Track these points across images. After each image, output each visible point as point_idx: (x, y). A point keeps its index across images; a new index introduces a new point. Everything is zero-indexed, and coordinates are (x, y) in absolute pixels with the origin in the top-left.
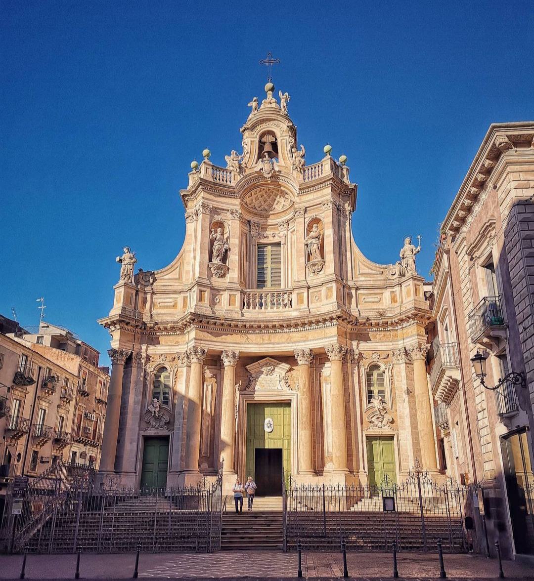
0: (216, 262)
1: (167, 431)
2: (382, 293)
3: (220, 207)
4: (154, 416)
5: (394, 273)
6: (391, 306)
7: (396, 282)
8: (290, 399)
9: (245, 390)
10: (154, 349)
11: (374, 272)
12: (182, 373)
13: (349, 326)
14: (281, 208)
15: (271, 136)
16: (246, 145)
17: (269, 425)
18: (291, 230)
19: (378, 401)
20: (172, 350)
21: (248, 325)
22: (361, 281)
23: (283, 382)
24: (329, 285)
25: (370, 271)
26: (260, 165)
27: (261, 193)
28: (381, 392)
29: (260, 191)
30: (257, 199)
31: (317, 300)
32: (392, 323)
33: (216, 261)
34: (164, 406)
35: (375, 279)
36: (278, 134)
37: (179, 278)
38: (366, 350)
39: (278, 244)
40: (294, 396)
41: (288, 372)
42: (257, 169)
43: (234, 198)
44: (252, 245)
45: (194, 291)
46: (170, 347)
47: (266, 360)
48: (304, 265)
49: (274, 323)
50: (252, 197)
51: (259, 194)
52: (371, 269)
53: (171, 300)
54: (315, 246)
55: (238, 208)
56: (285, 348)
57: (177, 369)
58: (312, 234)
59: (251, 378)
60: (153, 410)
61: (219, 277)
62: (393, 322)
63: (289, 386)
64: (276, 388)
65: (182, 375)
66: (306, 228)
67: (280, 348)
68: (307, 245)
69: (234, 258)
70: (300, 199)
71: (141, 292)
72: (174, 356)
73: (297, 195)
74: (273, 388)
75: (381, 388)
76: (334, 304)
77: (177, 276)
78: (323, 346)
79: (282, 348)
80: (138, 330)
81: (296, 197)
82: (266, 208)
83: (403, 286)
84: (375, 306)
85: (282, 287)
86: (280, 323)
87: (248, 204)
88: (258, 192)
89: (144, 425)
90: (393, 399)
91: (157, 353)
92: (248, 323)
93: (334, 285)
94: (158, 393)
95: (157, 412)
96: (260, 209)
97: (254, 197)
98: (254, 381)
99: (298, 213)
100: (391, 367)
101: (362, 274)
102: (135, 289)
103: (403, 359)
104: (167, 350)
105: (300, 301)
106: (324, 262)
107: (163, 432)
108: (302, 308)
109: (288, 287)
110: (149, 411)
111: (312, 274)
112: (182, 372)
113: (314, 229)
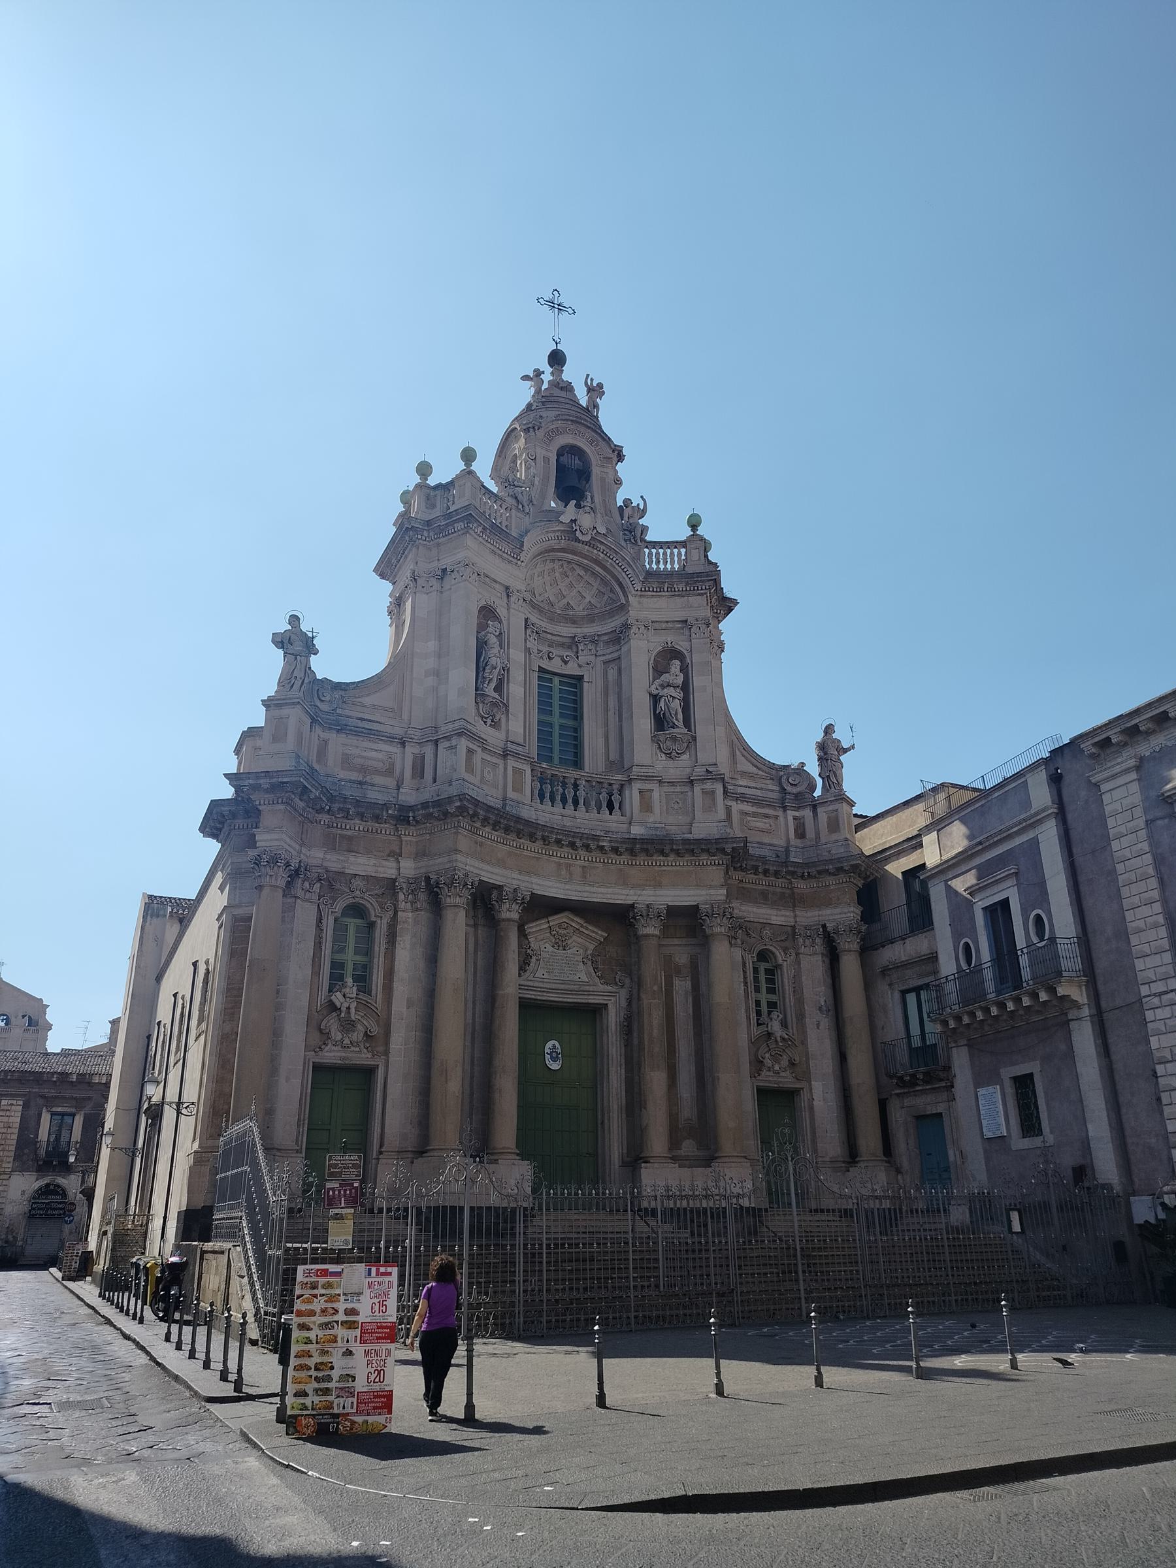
1: (369, 1055)
3: (493, 576)
8: (605, 1002)
11: (760, 773)
14: (581, 608)
15: (577, 458)
17: (554, 1055)
18: (604, 658)
20: (380, 869)
22: (741, 786)
25: (754, 770)
33: (489, 690)
35: (764, 786)
52: (756, 766)
53: (380, 756)
56: (613, 896)
57: (391, 913)
58: (665, 677)
60: (346, 1005)
66: (652, 661)
68: (655, 699)
74: (571, 978)
75: (773, 998)
76: (711, 824)
78: (696, 904)
83: (820, 810)
86: (613, 844)
89: (316, 1038)
91: (347, 871)
95: (353, 1010)
96: (541, 599)
98: (534, 959)
101: (744, 774)
103: (820, 946)
105: (646, 806)
106: (694, 738)
107: (363, 1058)
108: (651, 820)
110: (332, 1007)
113: (673, 670)
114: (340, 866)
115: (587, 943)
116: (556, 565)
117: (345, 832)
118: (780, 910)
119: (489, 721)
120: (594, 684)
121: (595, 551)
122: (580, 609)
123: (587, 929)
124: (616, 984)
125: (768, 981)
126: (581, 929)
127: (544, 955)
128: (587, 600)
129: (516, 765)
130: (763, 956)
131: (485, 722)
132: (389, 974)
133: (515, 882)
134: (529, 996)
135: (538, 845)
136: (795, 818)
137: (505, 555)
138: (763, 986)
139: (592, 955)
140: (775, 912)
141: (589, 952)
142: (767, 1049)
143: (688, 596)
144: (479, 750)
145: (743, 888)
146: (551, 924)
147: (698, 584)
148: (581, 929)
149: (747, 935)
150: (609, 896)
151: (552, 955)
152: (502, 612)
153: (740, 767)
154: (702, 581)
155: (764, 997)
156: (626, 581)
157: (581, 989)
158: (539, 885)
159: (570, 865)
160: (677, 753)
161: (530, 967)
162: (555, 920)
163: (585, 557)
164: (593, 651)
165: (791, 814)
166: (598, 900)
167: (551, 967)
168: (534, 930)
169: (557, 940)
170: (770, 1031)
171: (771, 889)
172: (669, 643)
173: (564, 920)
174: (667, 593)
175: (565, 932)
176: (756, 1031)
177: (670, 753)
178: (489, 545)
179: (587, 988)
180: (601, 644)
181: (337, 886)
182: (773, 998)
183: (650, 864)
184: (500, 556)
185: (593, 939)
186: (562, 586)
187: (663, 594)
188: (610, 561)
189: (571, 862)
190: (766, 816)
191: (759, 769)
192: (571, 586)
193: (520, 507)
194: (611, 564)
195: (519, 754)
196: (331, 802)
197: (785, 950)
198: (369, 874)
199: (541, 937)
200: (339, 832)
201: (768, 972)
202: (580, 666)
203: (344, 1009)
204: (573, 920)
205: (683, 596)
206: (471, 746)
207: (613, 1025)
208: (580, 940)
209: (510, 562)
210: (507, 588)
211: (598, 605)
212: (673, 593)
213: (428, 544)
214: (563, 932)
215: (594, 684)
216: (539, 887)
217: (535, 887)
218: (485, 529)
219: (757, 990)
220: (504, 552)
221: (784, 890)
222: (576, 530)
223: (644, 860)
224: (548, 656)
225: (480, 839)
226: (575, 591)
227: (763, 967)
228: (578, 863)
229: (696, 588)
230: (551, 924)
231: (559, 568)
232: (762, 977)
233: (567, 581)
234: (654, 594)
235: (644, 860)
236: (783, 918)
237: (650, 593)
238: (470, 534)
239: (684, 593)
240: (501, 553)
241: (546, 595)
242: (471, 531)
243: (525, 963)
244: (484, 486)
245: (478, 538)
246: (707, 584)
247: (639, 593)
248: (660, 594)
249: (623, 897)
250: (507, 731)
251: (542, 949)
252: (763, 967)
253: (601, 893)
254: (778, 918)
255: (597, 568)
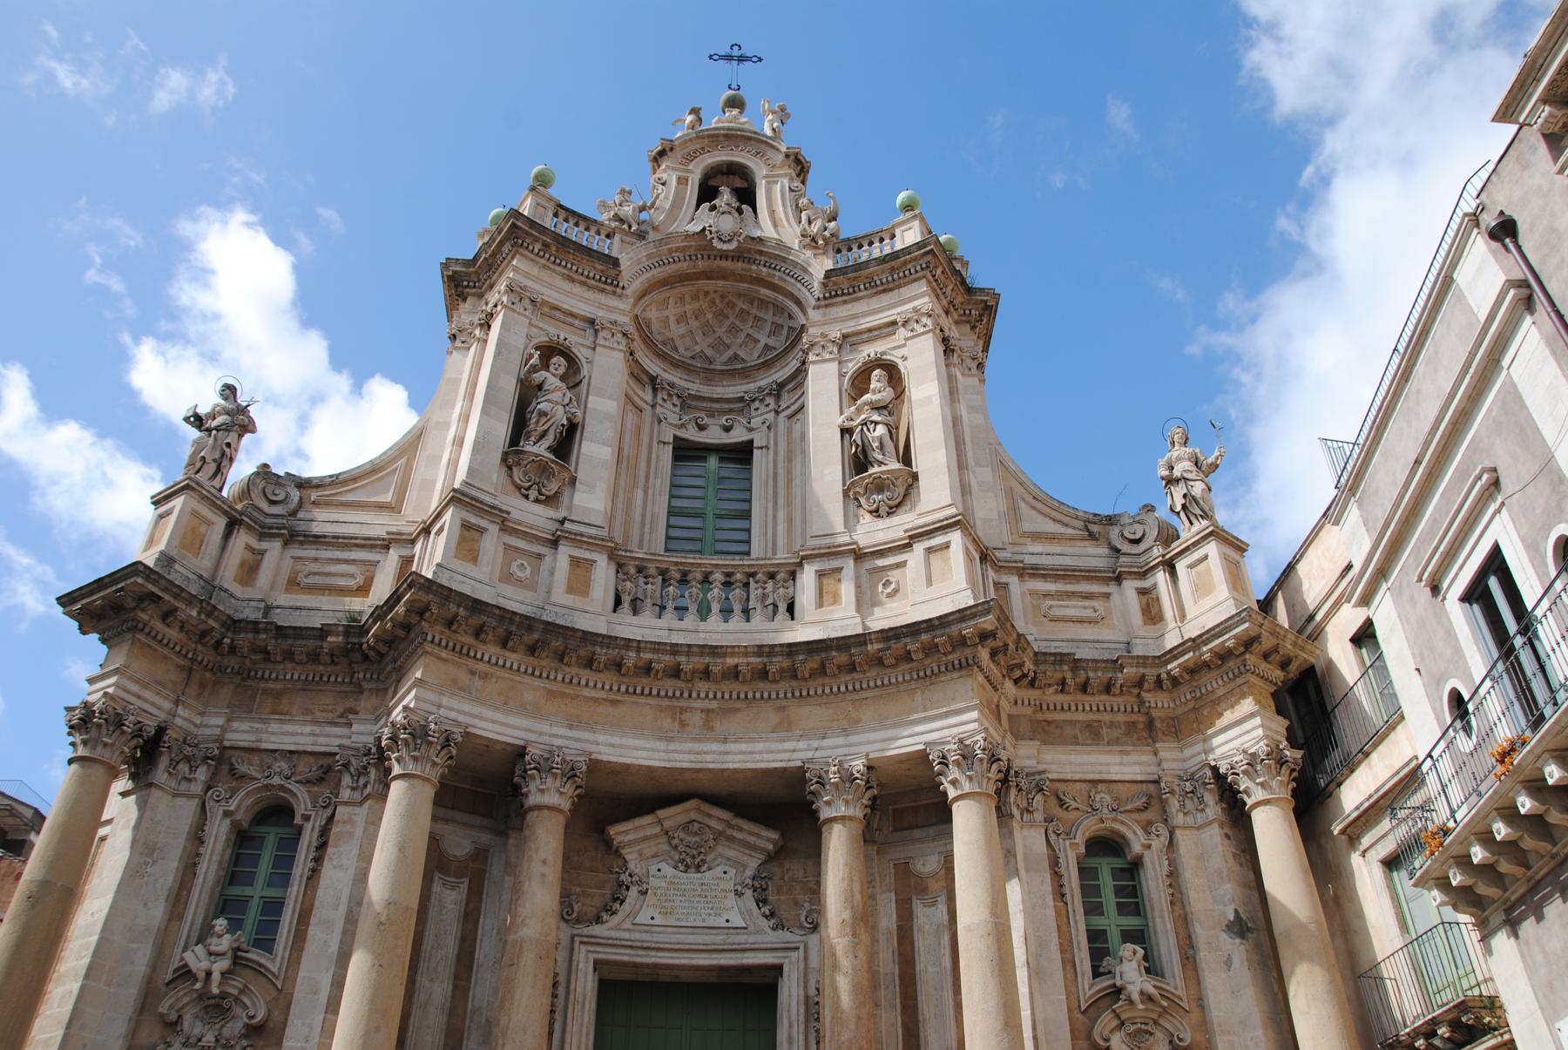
0: (535, 449)
2: (1107, 596)
4: (204, 995)
5: (1137, 536)
6: (1141, 633)
7: (1157, 551)
9: (598, 920)
10: (257, 731)
11: (1070, 531)
12: (348, 827)
13: (1009, 685)
14: (755, 356)
16: (663, 184)
19: (1134, 964)
20: (322, 740)
21: (631, 658)
23: (749, 898)
24: (938, 540)
25: (1058, 528)
26: (705, 219)
27: (696, 305)
28: (1137, 936)
29: (695, 297)
30: (682, 318)
31: (889, 596)
32: (1159, 682)
33: (539, 449)
34: (255, 955)
36: (759, 171)
37: (393, 508)
38: (1069, 777)
39: (742, 454)
40: (794, 955)
41: (772, 858)
42: (695, 227)
43: (614, 293)
44: (659, 442)
45: (441, 530)
46: (317, 729)
47: (687, 811)
48: (839, 488)
49: (730, 661)
50: (667, 313)
51: (690, 307)
54: (881, 430)
55: (625, 320)
56: (766, 756)
57: (329, 811)
59: (624, 877)
60: (205, 964)
61: (537, 501)
62: (1164, 676)
63: (772, 915)
64: (721, 922)
65: (351, 835)
67: (749, 757)
68: (846, 432)
69: (594, 451)
70: (824, 315)
71: (250, 528)
72: (326, 761)
73: (813, 303)
74: (711, 922)
77: (387, 497)
78: (921, 747)
79: (757, 757)
80: (206, 655)
81: (811, 312)
82: (709, 352)
83: (1180, 566)
84: (1087, 632)
85: (757, 549)
87: (654, 328)
88: (688, 298)
90: (1189, 958)
91: (265, 746)
92: (632, 654)
93: (956, 537)
94: (244, 902)
95: (216, 976)
96: (689, 354)
97: (672, 312)
98: (634, 891)
99: (817, 349)
100: (1164, 839)
101: (1037, 537)
102: (225, 513)
103: (1213, 808)
104: (302, 740)
106: (915, 477)
108: (836, 616)
109: (774, 553)
110: (185, 973)
111: (868, 516)
112: (349, 821)
114: (253, 739)
115: (745, 858)
116: (703, 303)
117: (271, 685)
118: (1127, 753)
119: (533, 494)
120: (771, 451)
121: (754, 267)
122: (752, 356)
123: (740, 829)
124: (802, 927)
125: (1118, 891)
126: (729, 832)
127: (654, 882)
128: (761, 344)
129: (578, 553)
130: (1106, 845)
131: (527, 497)
132: (304, 917)
133: (546, 739)
134: (618, 958)
135: (609, 678)
136: (1142, 592)
137: (592, 282)
138: (1109, 899)
139: (754, 878)
140: (1117, 759)
141: (749, 872)
142: (1115, 1023)
143: (899, 287)
144: (493, 529)
145: (1049, 722)
146: (667, 824)
147: (909, 266)
148: (729, 832)
149: (1062, 806)
150: (757, 757)
151: (672, 883)
152: (581, 353)
153: (1027, 527)
154: (915, 259)
155: (1112, 922)
156: (804, 294)
157: (730, 941)
158: (612, 745)
159: (683, 710)
160: (891, 508)
161: (626, 906)
162: (672, 816)
163: (742, 279)
164: (772, 406)
165: (1130, 586)
166: (737, 766)
167: (670, 904)
168: (631, 837)
169: (684, 855)
170: (1118, 983)
171: (1106, 717)
172: (872, 355)
173: (693, 816)
174: (865, 293)
175: (697, 839)
176: (1088, 988)
177: (877, 511)
178: (558, 269)
179: (743, 938)
180: (785, 396)
181: (243, 768)
182: (1131, 922)
183: (835, 689)
184: (583, 284)
185: (754, 848)
186: (721, 331)
187: (861, 294)
188: (778, 274)
189: (683, 703)
190: (1088, 596)
191: (1066, 525)
192: (734, 330)
193: (625, 226)
194: (780, 278)
195: (582, 535)
196: (235, 632)
197: (1147, 827)
198: (301, 748)
199: (648, 852)
200: (262, 685)
201: (1117, 873)
202: (750, 430)
203: (202, 975)
204: (710, 816)
205: (891, 290)
206: (474, 520)
207: (794, 1004)
208: (731, 853)
209: (603, 291)
210: (592, 322)
211: (776, 345)
212: (875, 290)
213: (479, 291)
214: (693, 839)
215: (771, 451)
216: (612, 750)
217: (602, 749)
218: (545, 245)
219: (1093, 909)
220: (588, 277)
221: (1134, 717)
222: (713, 238)
223: (823, 686)
224: (697, 423)
225: (481, 667)
226: (742, 336)
227: (1105, 868)
228: (698, 704)
229: (907, 272)
230: (667, 824)
231: (711, 307)
232: (1107, 883)
233: (728, 323)
234: (845, 298)
235: (823, 686)
236: (1137, 769)
237: (839, 299)
238: (522, 255)
239: (891, 285)
240: (583, 279)
241: (698, 349)
242: (521, 250)
243: (615, 900)
244: (561, 206)
245: (537, 259)
246: (923, 262)
247: (823, 303)
248: (855, 295)
249: (786, 756)
250: (570, 508)
251: (653, 869)
252: (1105, 868)
253: (741, 753)
254: (1127, 769)
255: (765, 292)
